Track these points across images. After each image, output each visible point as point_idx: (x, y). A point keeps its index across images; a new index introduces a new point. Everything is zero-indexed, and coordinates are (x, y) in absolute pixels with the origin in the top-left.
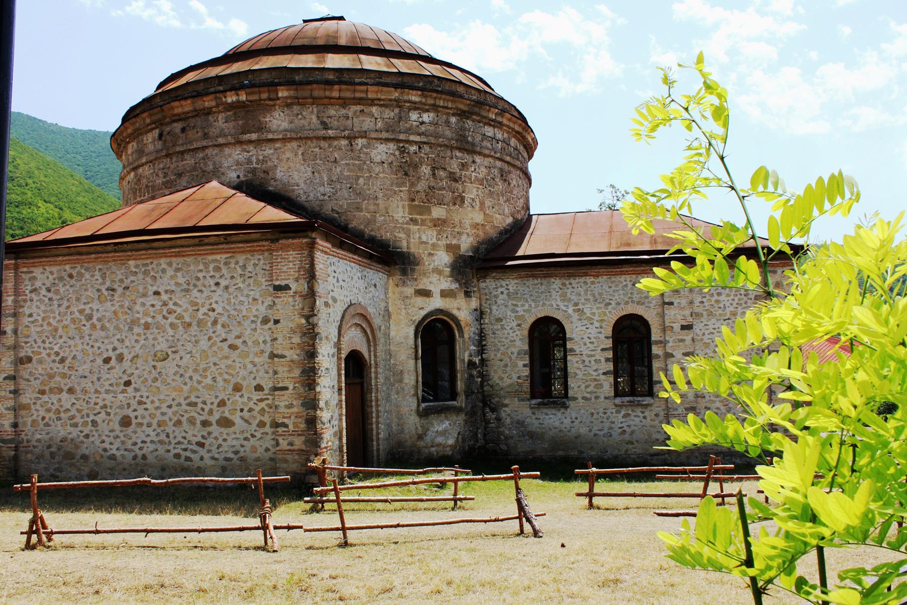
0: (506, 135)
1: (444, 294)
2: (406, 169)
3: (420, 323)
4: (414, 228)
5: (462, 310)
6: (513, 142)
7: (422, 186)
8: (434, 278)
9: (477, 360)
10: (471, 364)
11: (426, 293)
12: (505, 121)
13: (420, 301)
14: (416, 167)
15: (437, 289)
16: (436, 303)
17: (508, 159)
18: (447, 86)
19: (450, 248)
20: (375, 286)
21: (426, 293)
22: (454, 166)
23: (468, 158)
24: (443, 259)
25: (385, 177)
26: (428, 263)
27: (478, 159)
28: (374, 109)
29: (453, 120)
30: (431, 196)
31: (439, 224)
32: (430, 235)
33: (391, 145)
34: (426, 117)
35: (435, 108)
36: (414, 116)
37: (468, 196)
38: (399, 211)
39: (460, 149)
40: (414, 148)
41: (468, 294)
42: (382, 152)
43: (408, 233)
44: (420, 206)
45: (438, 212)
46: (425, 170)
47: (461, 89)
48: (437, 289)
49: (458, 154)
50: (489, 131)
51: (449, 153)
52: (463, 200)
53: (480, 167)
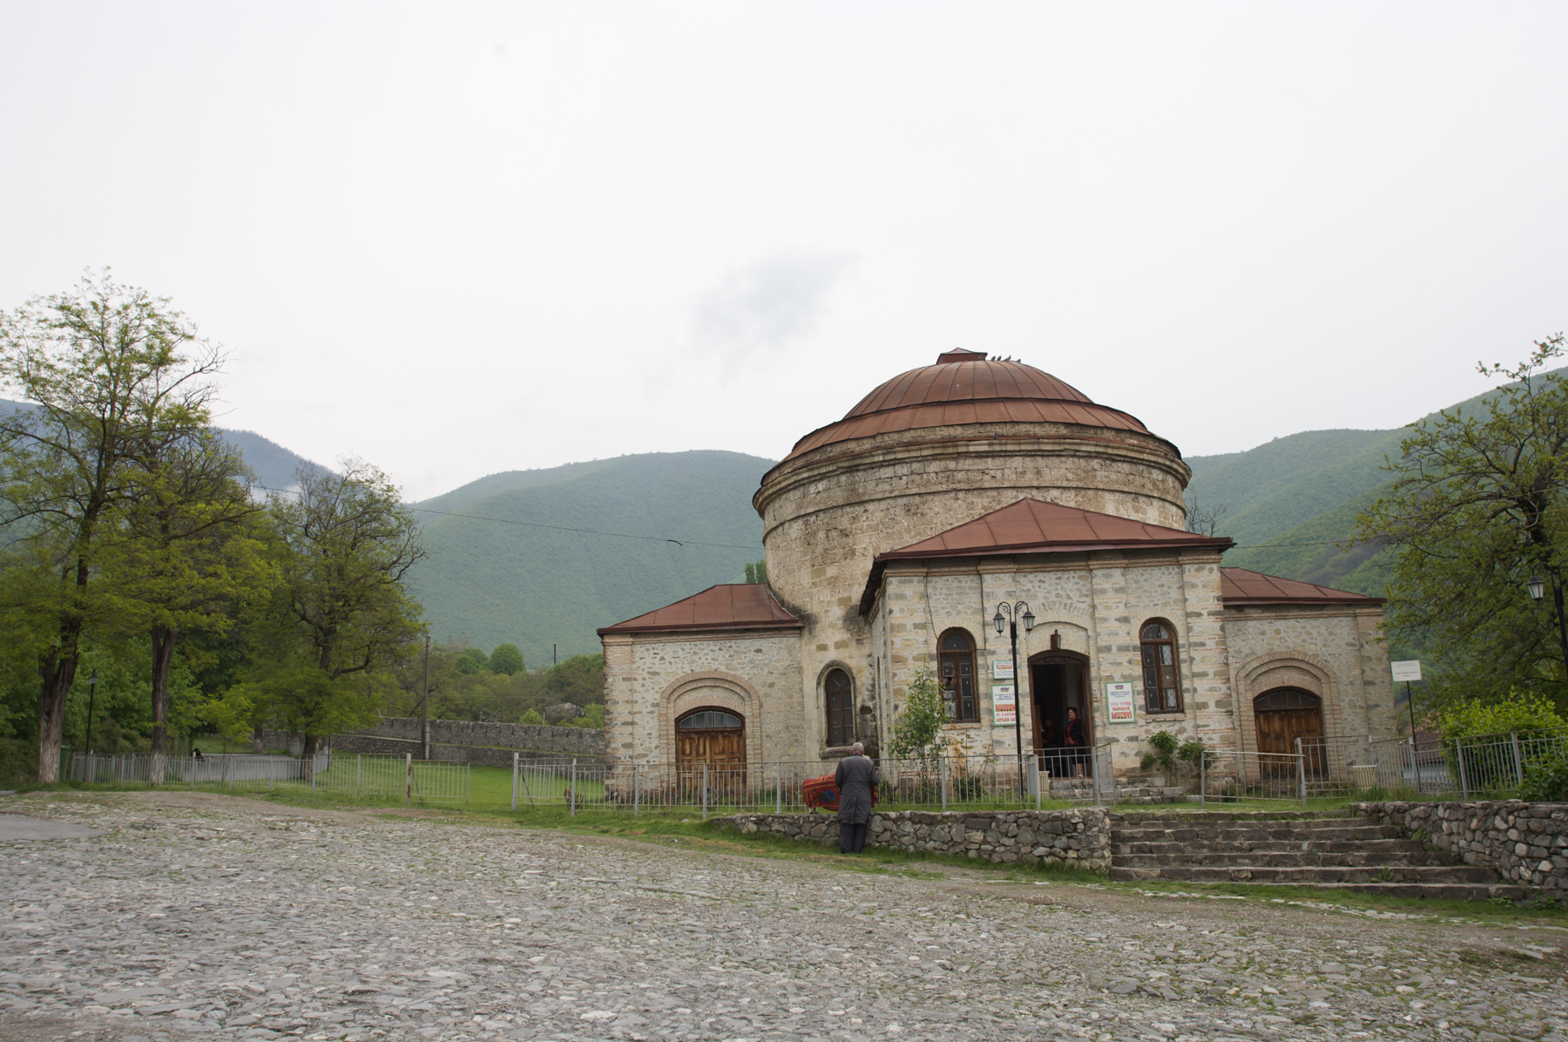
0: (916, 466)
1: (838, 645)
2: (808, 540)
3: (822, 673)
4: (814, 590)
5: (854, 659)
6: (934, 466)
7: (819, 550)
8: (830, 632)
9: (870, 704)
10: (865, 710)
11: (822, 648)
12: (900, 456)
13: (820, 655)
14: (815, 534)
15: (831, 641)
16: (832, 655)
17: (914, 491)
18: (837, 450)
19: (842, 602)
20: (759, 651)
21: (822, 648)
22: (845, 522)
23: (860, 509)
24: (837, 612)
25: (798, 548)
26: (825, 621)
27: (870, 507)
28: (791, 495)
29: (843, 478)
30: (826, 558)
31: (833, 581)
32: (825, 594)
33: (800, 522)
34: (821, 486)
35: (822, 477)
36: (812, 489)
37: (859, 548)
38: (805, 577)
39: (850, 505)
40: (813, 518)
41: (859, 642)
42: (796, 529)
43: (811, 596)
44: (818, 571)
45: (831, 571)
46: (821, 535)
47: (852, 446)
48: (831, 641)
49: (848, 509)
50: (887, 472)
51: (839, 512)
52: (853, 552)
53: (876, 512)
